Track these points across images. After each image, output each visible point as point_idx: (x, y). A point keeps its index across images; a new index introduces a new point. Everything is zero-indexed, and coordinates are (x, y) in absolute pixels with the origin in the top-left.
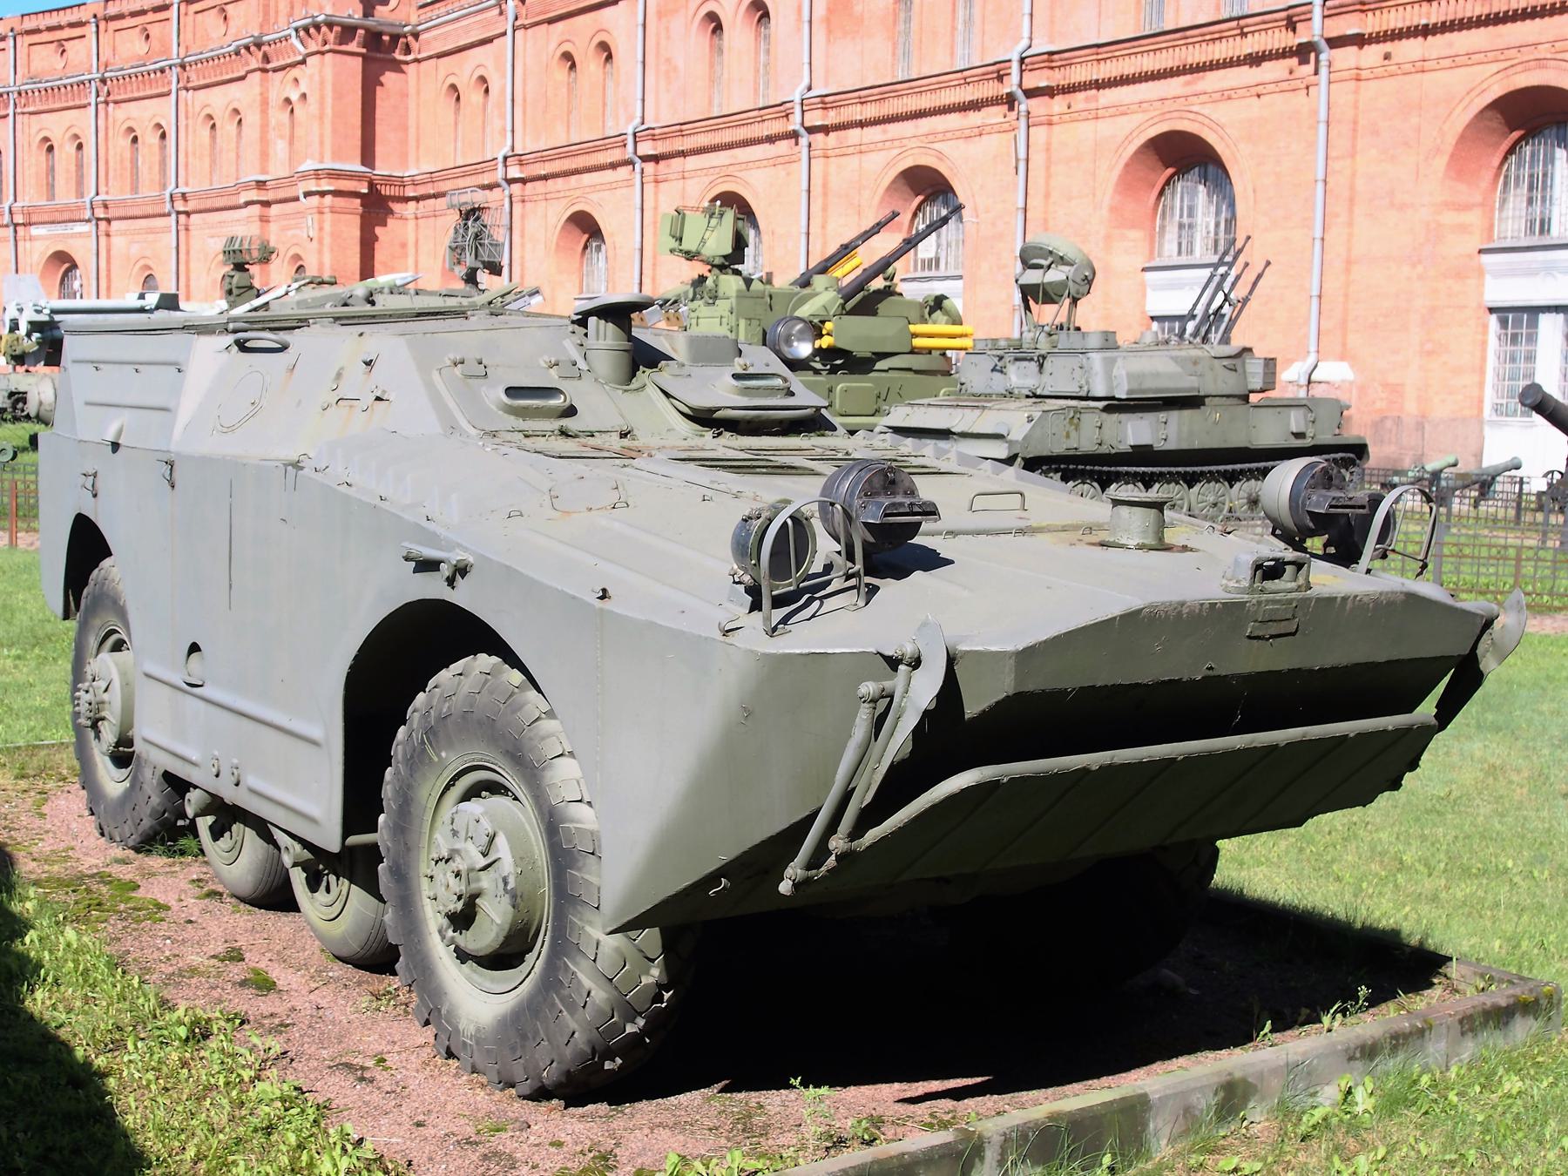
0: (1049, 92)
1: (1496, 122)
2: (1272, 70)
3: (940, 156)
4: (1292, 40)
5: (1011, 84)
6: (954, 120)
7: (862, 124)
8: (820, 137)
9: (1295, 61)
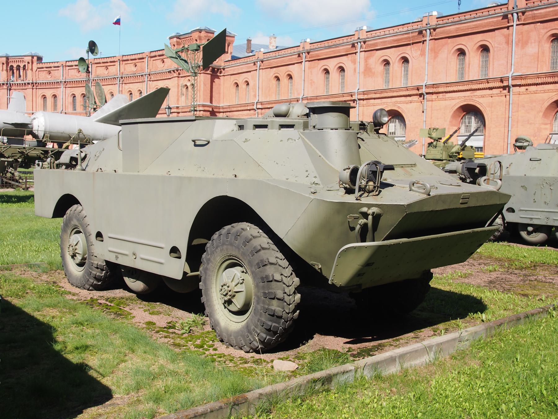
0: (432, 93)
1: (555, 105)
2: (495, 91)
3: (399, 107)
4: (501, 85)
5: (424, 90)
6: (403, 99)
7: (374, 99)
8: (362, 101)
9: (502, 89)
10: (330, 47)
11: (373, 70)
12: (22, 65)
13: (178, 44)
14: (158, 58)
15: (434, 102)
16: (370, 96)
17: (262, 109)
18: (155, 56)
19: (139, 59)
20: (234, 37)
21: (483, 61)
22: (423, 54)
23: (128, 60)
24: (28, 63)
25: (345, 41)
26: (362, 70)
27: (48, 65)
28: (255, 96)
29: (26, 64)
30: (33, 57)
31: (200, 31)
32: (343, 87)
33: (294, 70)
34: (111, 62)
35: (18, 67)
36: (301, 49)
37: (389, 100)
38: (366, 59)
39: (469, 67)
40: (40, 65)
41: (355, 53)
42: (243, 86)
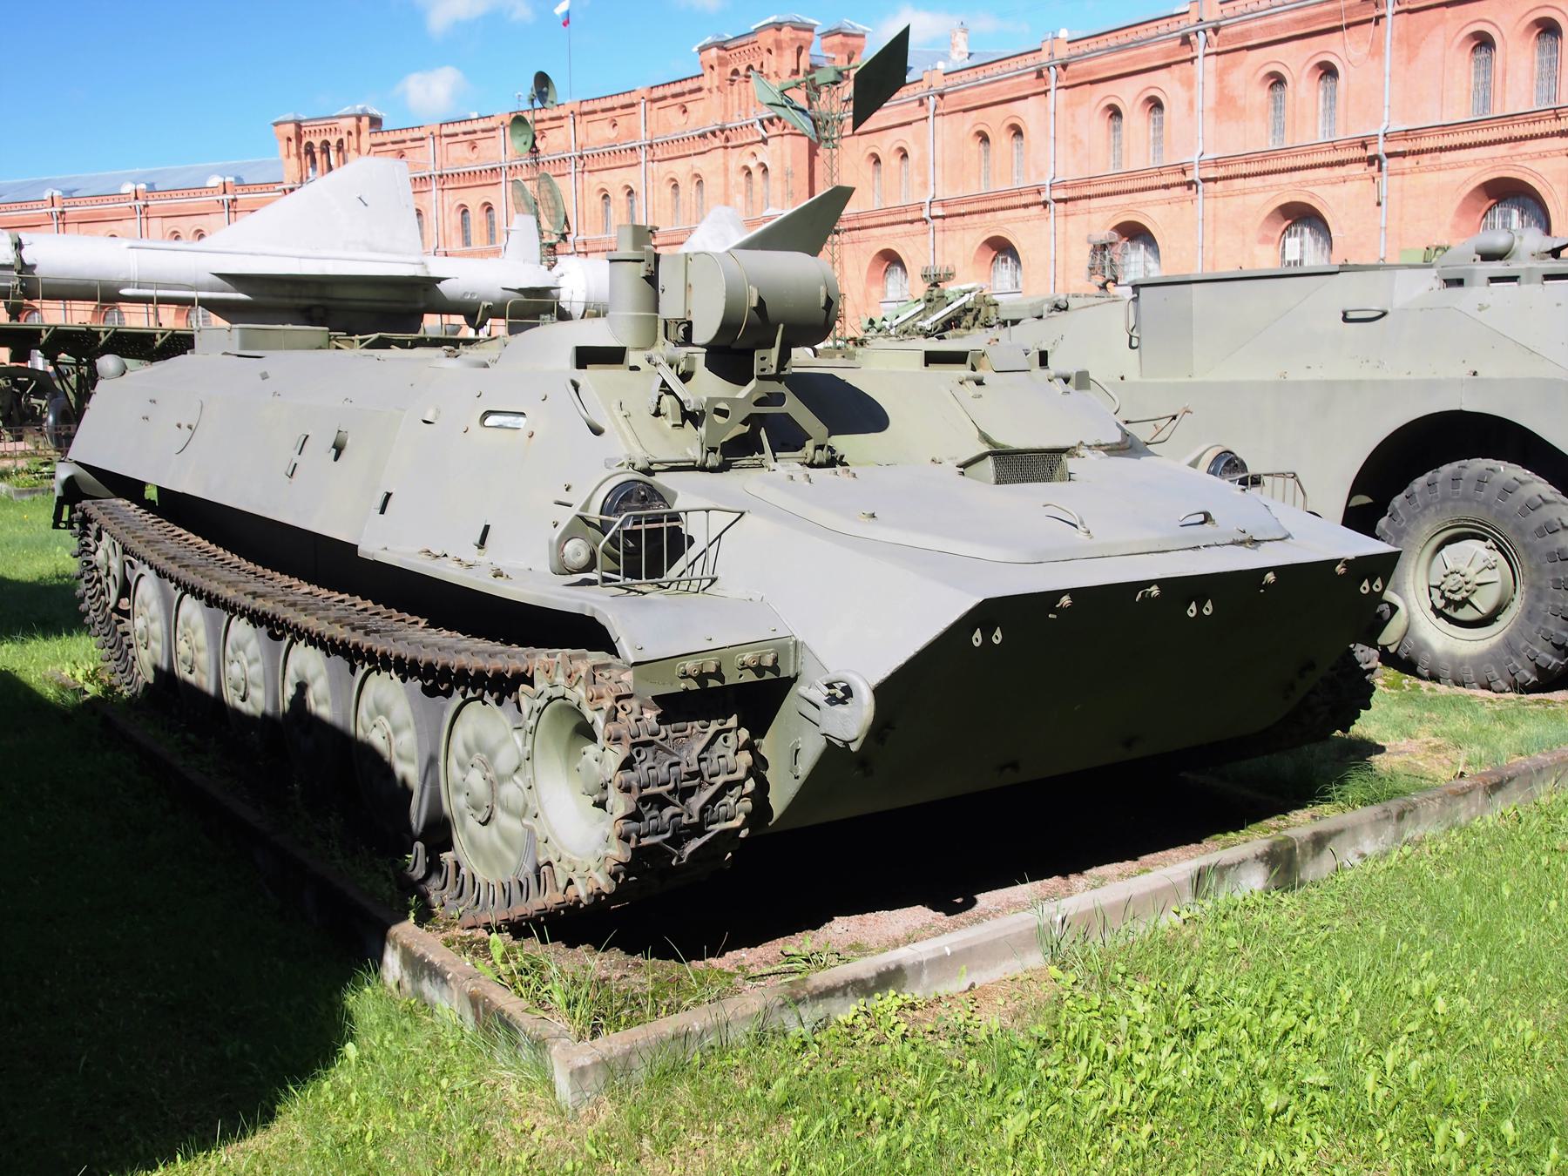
0: (1403, 154)
3: (1312, 195)
5: (1380, 148)
6: (1322, 173)
8: (1211, 184)
10: (1121, 48)
11: (1241, 102)
12: (333, 140)
13: (723, 62)
14: (670, 101)
15: (1407, 177)
16: (1232, 171)
17: (944, 217)
18: (664, 98)
19: (623, 107)
20: (863, 36)
21: (1541, 62)
22: (1376, 51)
23: (594, 112)
24: (350, 133)
25: (1163, 29)
26: (1210, 101)
27: (398, 136)
28: (925, 185)
29: (344, 136)
30: (359, 118)
31: (778, 27)
32: (1159, 150)
33: (1027, 112)
34: (552, 119)
35: (326, 143)
36: (1044, 58)
37: (1285, 177)
38: (1221, 75)
39: (1504, 80)
40: (379, 138)
41: (1192, 60)
42: (891, 161)
